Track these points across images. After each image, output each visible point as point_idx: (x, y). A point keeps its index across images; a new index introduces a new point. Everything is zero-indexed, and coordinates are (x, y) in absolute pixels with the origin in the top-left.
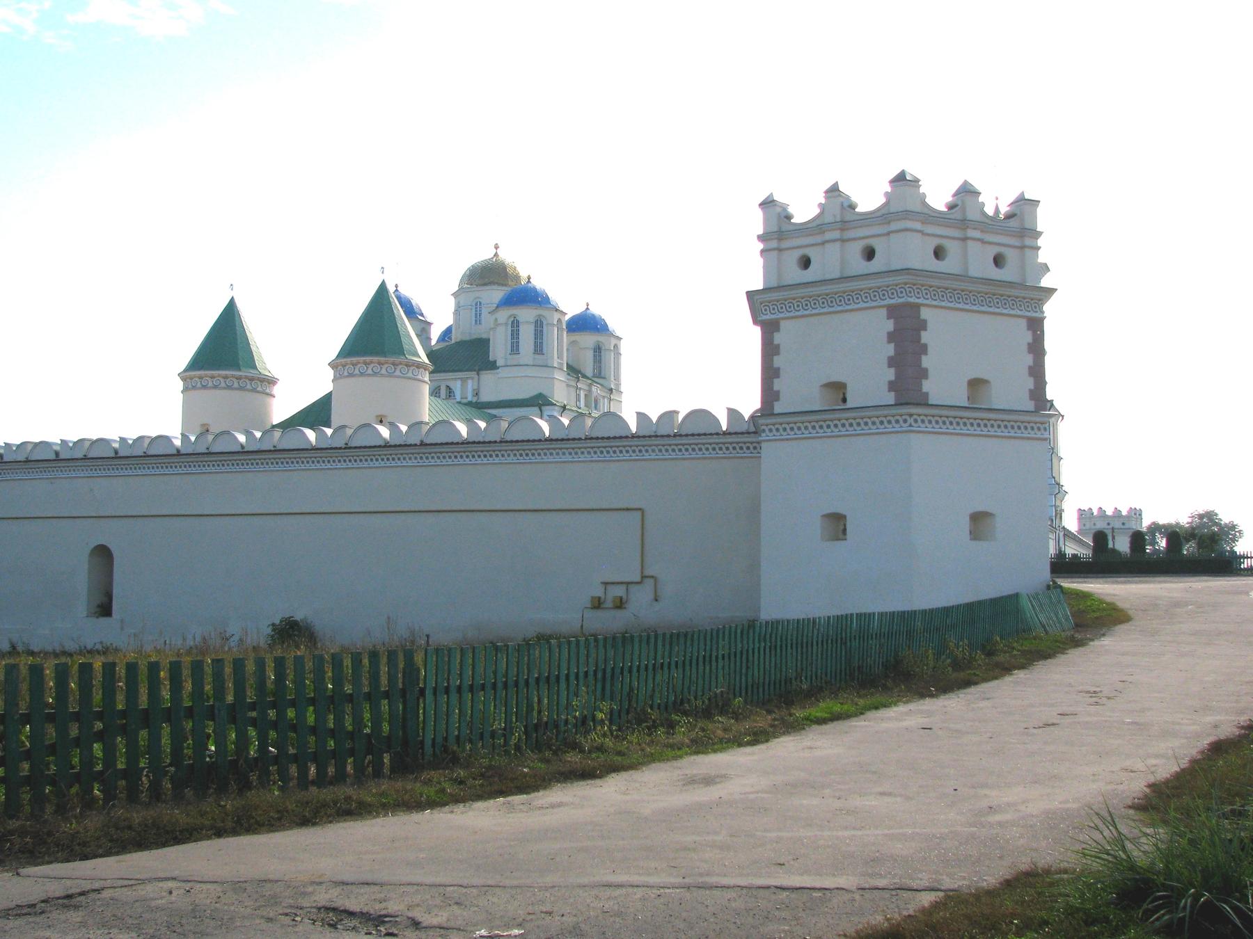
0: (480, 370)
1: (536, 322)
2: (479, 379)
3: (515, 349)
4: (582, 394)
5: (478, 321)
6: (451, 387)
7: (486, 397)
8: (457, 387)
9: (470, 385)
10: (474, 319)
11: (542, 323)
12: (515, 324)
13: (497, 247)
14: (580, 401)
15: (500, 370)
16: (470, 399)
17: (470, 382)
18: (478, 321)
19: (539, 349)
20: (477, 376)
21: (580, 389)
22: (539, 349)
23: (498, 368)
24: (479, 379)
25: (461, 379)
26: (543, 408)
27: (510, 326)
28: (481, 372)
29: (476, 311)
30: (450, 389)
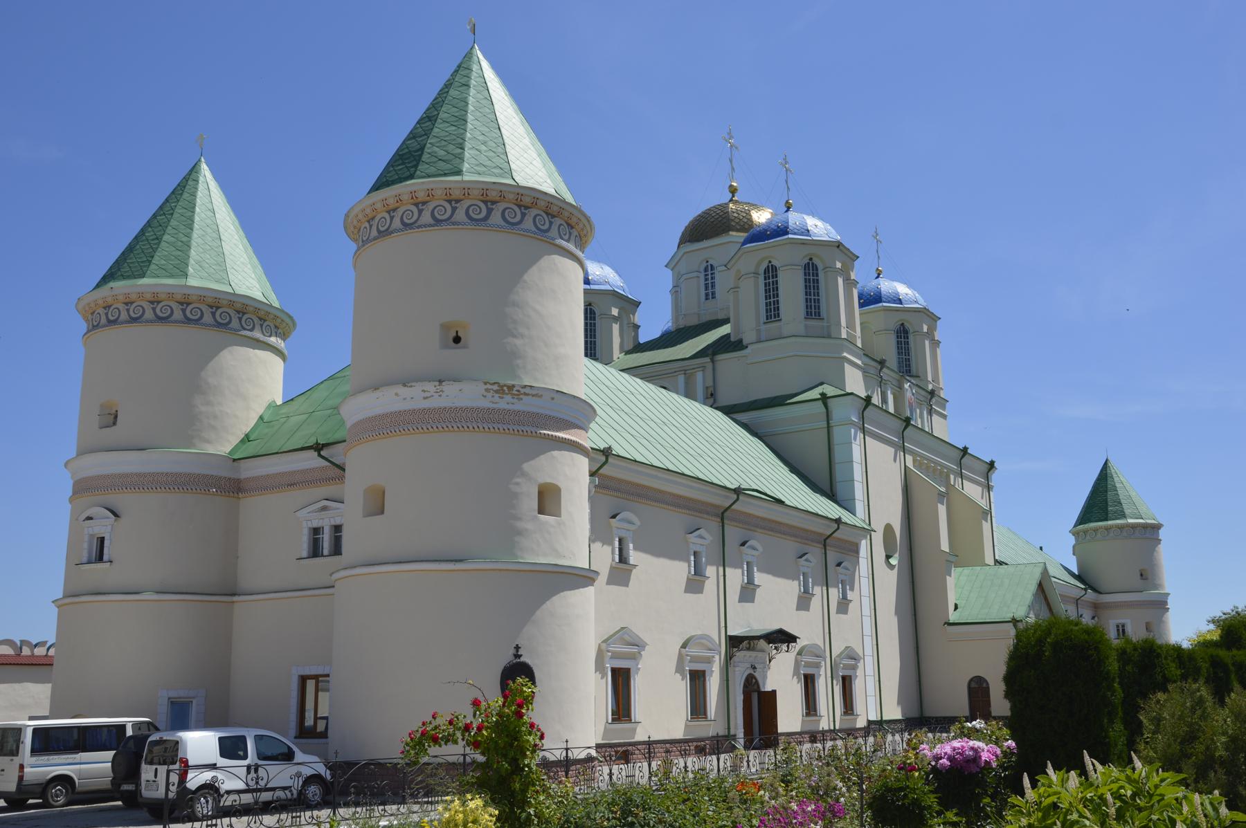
0: (714, 354)
1: (806, 267)
2: (714, 369)
3: (773, 312)
5: (710, 295)
10: (703, 292)
11: (815, 268)
12: (771, 272)
13: (733, 191)
17: (699, 376)
18: (710, 295)
19: (814, 308)
20: (710, 366)
23: (747, 347)
24: (714, 369)
26: (831, 403)
27: (762, 277)
28: (719, 357)
29: (706, 280)
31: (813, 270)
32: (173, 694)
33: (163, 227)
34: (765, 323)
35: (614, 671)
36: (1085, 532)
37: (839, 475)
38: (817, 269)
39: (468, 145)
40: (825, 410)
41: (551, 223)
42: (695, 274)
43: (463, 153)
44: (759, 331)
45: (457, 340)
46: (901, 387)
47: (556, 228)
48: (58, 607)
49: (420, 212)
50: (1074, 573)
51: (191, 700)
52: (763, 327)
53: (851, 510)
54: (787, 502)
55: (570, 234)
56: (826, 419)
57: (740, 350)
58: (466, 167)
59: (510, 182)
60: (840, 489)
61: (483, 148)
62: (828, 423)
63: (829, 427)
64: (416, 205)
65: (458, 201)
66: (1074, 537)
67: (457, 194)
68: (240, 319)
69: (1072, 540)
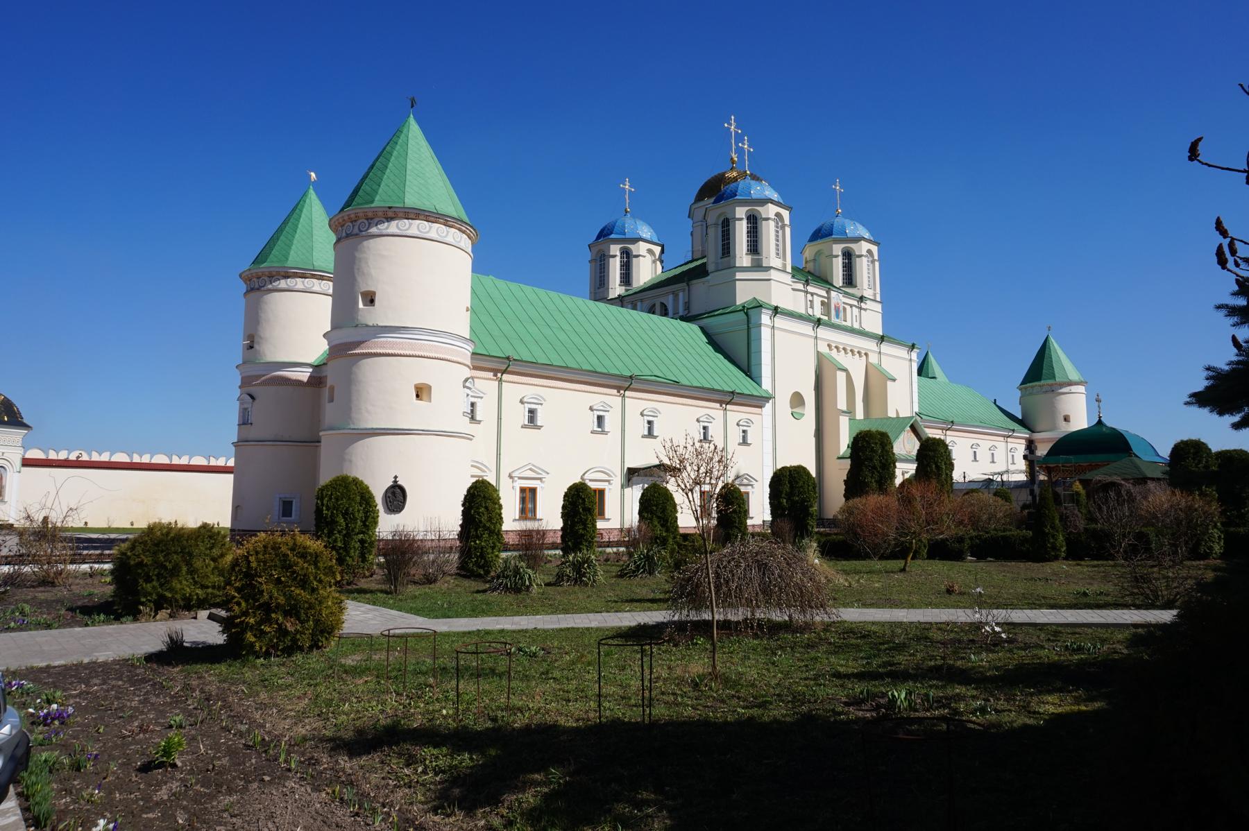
4: (817, 301)
6: (665, 302)
7: (694, 311)
8: (669, 301)
9: (682, 297)
14: (812, 307)
15: (709, 277)
16: (681, 314)
17: (681, 294)
20: (687, 288)
21: (812, 294)
22: (754, 248)
25: (673, 293)
27: (720, 227)
28: (695, 281)
30: (665, 306)
31: (753, 219)
32: (282, 496)
33: (282, 231)
34: (721, 258)
35: (523, 490)
36: (1026, 388)
37: (753, 362)
38: (756, 219)
39: (383, 184)
40: (746, 317)
41: (430, 227)
42: (699, 223)
43: (378, 189)
44: (717, 263)
45: (372, 302)
46: (829, 298)
47: (435, 230)
48: (235, 446)
49: (353, 226)
50: (1018, 418)
51: (291, 500)
52: (720, 261)
53: (760, 384)
54: (684, 382)
55: (448, 232)
56: (746, 322)
57: (707, 276)
58: (377, 198)
59: (401, 205)
60: (753, 369)
61: (392, 185)
62: (748, 326)
63: (749, 328)
64: (352, 222)
65: (372, 219)
66: (1020, 392)
67: (370, 215)
68: (320, 284)
69: (1019, 393)
